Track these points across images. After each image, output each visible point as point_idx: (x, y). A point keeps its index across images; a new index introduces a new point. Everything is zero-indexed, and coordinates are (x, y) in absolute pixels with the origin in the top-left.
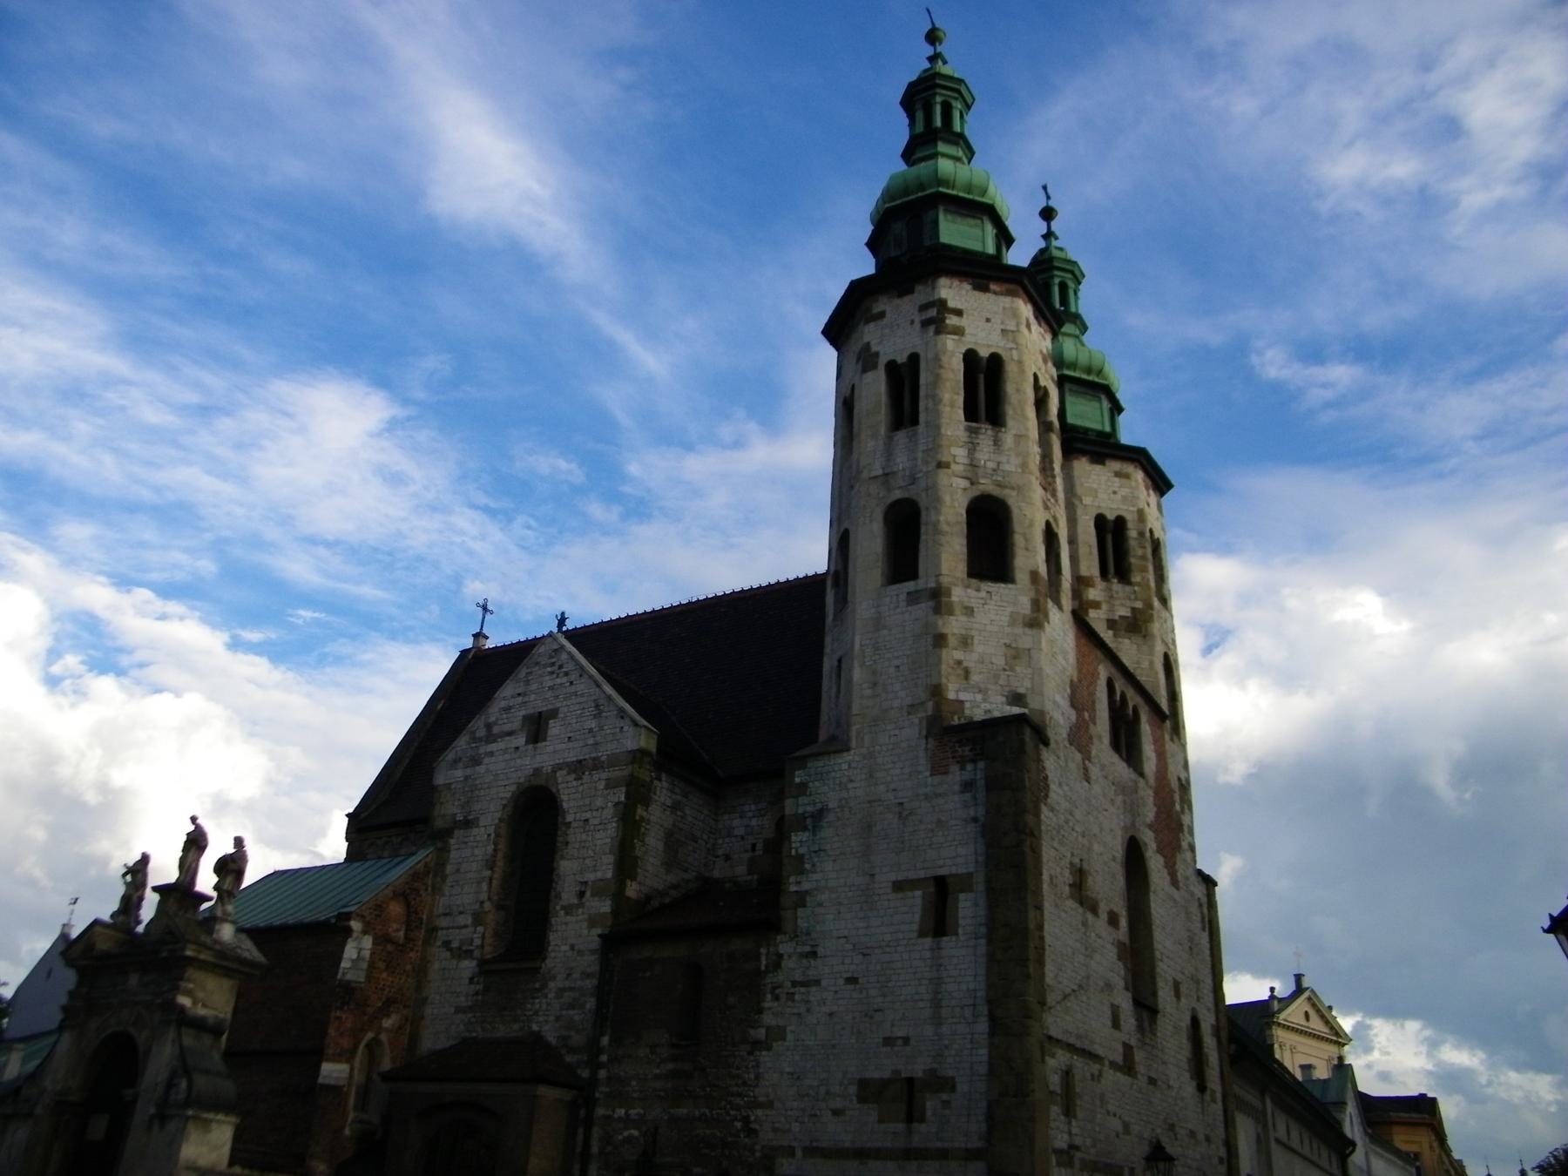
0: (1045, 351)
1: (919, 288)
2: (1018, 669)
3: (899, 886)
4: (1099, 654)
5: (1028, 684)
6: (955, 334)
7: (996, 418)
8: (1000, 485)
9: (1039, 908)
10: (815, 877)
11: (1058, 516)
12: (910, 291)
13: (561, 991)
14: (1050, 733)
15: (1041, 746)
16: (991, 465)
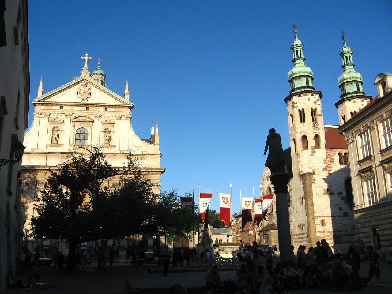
0: (315, 100)
1: (291, 99)
2: (310, 163)
3: (299, 198)
4: (335, 150)
5: (311, 165)
6: (296, 107)
7: (304, 121)
8: (305, 133)
9: (312, 200)
10: (292, 198)
11: (319, 132)
12: (290, 101)
13: (275, 216)
14: (316, 172)
15: (313, 175)
16: (303, 130)
